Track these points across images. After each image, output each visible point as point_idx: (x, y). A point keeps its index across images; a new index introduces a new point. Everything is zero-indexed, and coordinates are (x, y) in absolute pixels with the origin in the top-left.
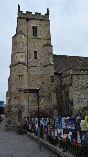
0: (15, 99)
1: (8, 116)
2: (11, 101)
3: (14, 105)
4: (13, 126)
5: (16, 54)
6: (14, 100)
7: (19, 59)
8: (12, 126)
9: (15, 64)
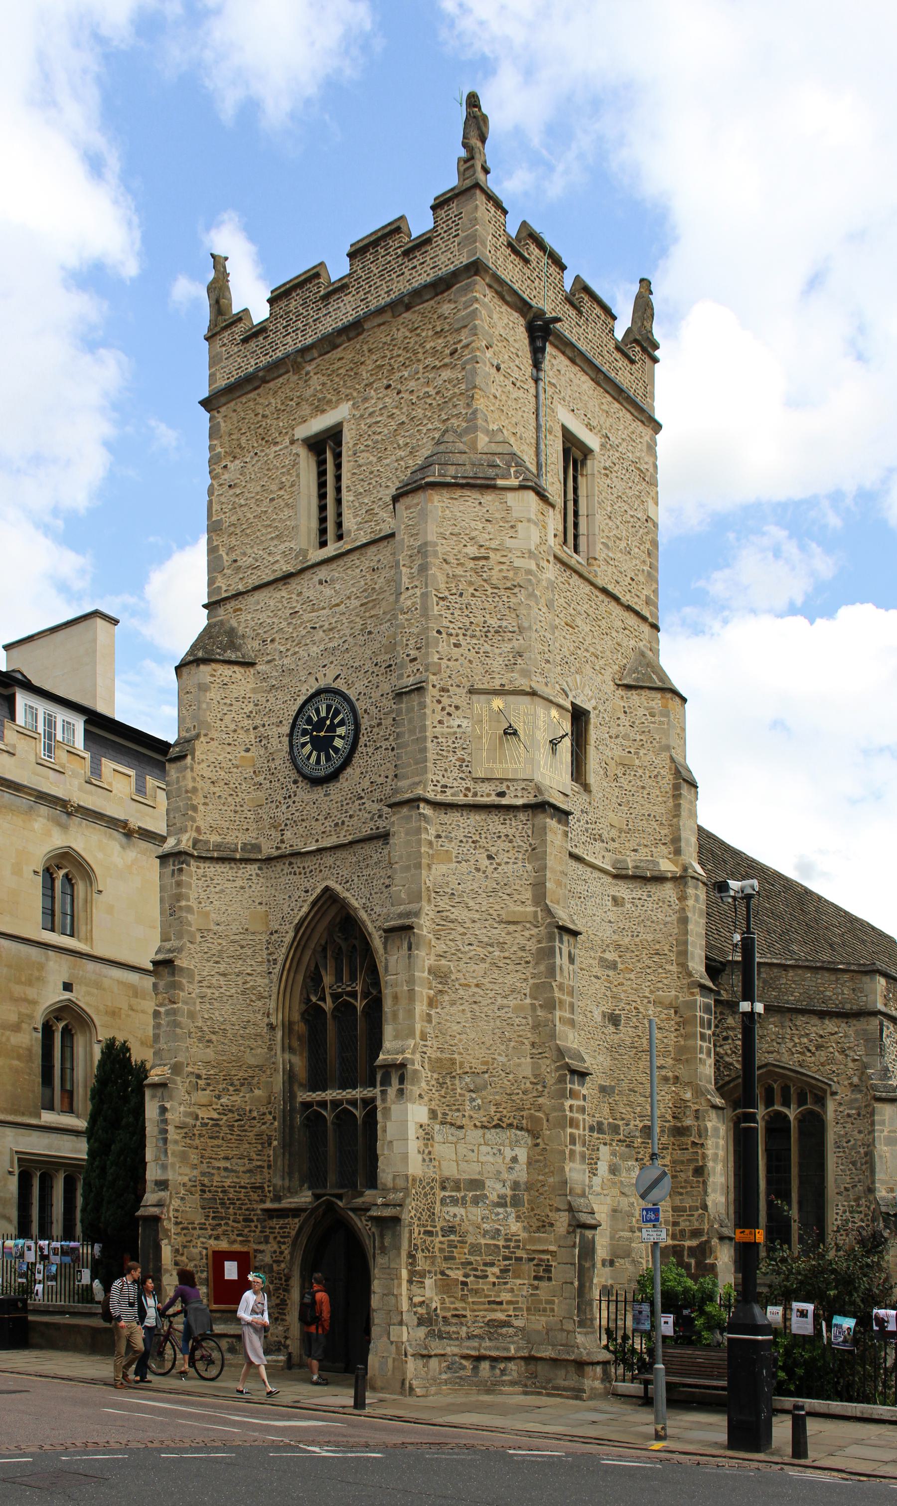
0: (491, 1135)
1: (422, 1274)
2: (438, 1138)
3: (476, 1184)
4: (479, 1359)
5: (500, 692)
6: (474, 1135)
7: (532, 761)
8: (465, 1357)
9: (487, 795)
